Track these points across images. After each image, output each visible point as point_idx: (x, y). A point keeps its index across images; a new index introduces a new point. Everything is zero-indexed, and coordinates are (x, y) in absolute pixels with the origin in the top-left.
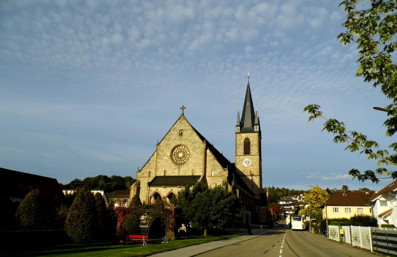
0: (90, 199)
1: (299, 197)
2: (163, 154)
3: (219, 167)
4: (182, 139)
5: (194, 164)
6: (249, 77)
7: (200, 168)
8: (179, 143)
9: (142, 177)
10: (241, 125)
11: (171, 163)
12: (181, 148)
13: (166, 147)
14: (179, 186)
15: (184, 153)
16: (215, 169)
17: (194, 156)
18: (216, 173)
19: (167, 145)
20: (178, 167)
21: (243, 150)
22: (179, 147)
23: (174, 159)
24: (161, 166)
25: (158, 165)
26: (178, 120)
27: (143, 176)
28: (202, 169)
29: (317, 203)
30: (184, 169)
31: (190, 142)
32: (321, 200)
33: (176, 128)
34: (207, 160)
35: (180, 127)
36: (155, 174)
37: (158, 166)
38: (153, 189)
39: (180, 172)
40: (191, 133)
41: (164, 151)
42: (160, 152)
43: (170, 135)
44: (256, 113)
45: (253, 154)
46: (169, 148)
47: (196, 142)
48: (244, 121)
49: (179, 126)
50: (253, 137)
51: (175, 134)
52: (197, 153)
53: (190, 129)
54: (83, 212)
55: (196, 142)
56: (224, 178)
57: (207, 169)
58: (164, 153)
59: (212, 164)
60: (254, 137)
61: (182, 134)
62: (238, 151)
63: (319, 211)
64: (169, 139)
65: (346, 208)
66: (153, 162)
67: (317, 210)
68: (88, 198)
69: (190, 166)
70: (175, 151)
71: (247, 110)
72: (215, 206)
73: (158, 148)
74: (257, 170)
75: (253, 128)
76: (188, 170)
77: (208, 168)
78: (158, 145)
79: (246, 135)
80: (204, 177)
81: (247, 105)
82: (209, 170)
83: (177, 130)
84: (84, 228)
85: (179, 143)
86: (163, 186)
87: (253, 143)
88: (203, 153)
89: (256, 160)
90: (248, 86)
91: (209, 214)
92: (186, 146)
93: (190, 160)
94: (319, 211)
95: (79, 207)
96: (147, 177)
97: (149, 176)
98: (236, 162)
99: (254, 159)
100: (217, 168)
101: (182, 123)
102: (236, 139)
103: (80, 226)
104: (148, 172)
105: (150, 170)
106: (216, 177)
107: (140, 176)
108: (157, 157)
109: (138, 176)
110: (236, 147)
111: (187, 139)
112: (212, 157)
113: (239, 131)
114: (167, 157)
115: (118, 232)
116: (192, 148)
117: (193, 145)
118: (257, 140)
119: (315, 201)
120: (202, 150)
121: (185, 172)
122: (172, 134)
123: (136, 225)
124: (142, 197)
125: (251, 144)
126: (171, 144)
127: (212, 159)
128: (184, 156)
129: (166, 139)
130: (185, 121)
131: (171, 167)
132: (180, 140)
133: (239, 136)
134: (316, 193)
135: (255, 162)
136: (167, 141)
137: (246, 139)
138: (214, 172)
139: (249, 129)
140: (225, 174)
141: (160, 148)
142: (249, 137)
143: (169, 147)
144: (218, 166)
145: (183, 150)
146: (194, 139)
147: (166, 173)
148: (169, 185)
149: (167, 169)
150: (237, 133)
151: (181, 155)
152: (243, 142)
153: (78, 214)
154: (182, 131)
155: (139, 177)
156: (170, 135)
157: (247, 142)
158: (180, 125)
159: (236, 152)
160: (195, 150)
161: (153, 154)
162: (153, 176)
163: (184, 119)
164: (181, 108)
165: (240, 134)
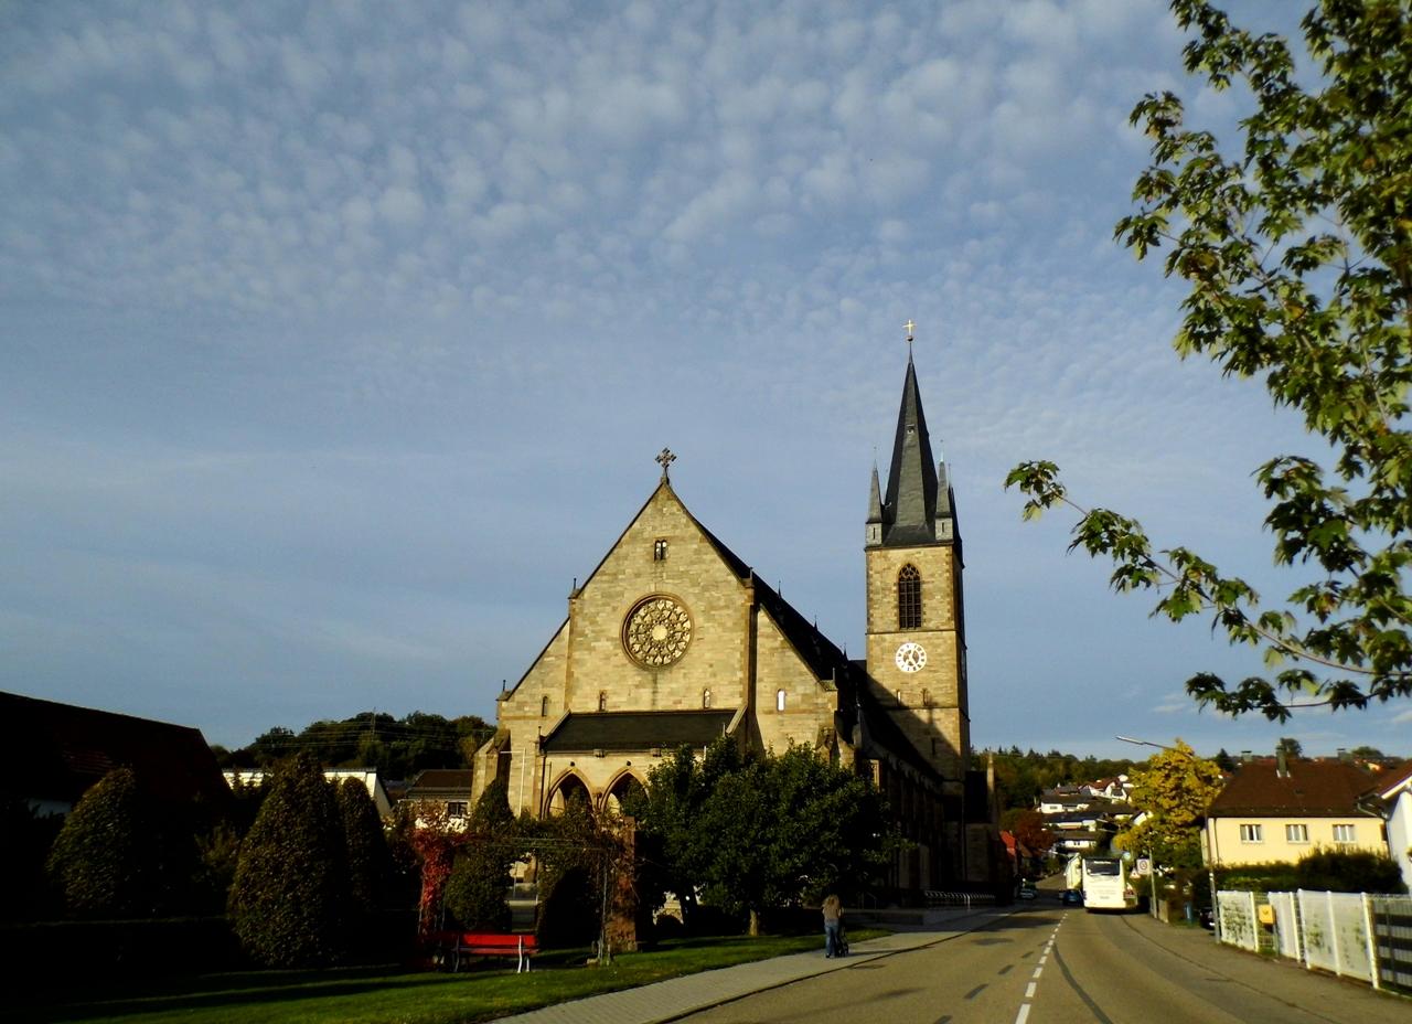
0: (321, 802)
1: (1113, 784)
2: (593, 631)
3: (803, 678)
4: (664, 575)
5: (711, 666)
6: (911, 340)
7: (731, 683)
8: (653, 590)
10: (887, 517)
12: (661, 606)
13: (604, 605)
14: (653, 751)
15: (672, 626)
16: (790, 684)
17: (707, 637)
18: (793, 698)
19: (607, 596)
20: (650, 677)
21: (896, 611)
22: (652, 605)
23: (637, 647)
24: (586, 675)
25: (577, 672)
26: (647, 504)
27: (519, 713)
29: (1178, 806)
30: (674, 686)
31: (693, 586)
32: (1197, 796)
33: (642, 533)
34: (760, 649)
35: (654, 528)
36: (566, 706)
37: (575, 675)
38: (560, 764)
39: (659, 696)
40: (697, 552)
41: (598, 619)
42: (580, 623)
43: (617, 559)
44: (942, 471)
45: (931, 625)
46: (614, 609)
47: (716, 585)
48: (895, 504)
49: (651, 527)
50: (931, 563)
51: (638, 553)
52: (722, 625)
53: (693, 537)
54: (294, 850)
55: (716, 585)
56: (822, 716)
57: (759, 686)
58: (598, 628)
59: (776, 666)
60: (937, 562)
61: (662, 556)
62: (876, 613)
63: (1188, 836)
64: (615, 574)
65: (1288, 826)
66: (558, 662)
67: (1181, 833)
68: (314, 797)
69: (696, 674)
70: (638, 620)
71: (905, 461)
72: (789, 821)
73: (574, 610)
74: (949, 685)
75: (933, 529)
76: (688, 689)
77: (761, 680)
78: (576, 597)
79: (907, 555)
80: (750, 716)
81: (908, 441)
82: (768, 689)
83: (645, 541)
84: (299, 912)
85: (652, 589)
86: (597, 752)
87: (930, 586)
88: (744, 624)
89: (943, 647)
90: (911, 374)
91: (767, 853)
92: (681, 600)
93: (694, 649)
94: (1188, 836)
95: (279, 834)
96: (535, 718)
97: (543, 715)
98: (868, 653)
99: (938, 646)
100: (797, 679)
102: (869, 569)
103: (283, 904)
104: (540, 698)
105: (546, 691)
106: (794, 712)
107: (511, 714)
108: (571, 642)
109: (503, 714)
110: (869, 599)
111: (681, 575)
112: (775, 638)
113: (878, 541)
114: (609, 643)
115: (423, 924)
116: (703, 608)
117: (707, 594)
118: (947, 571)
119: (1173, 798)
120: (739, 614)
123: (493, 897)
124: (517, 793)
125: (924, 586)
126: (622, 594)
128: (671, 637)
129: (604, 574)
130: (675, 508)
131: (624, 677)
132: (658, 577)
133: (879, 557)
134: (1176, 769)
135: (940, 655)
136: (608, 582)
137: (904, 569)
138: (786, 694)
139: (917, 532)
140: (826, 700)
141: (582, 609)
142: (915, 562)
143: (615, 605)
144: (801, 674)
145: (666, 613)
146: (707, 571)
147: (608, 701)
148: (619, 748)
149: (608, 688)
150: (869, 548)
151: (660, 633)
152: (895, 580)
153: (274, 859)
154: (664, 545)
155: (507, 719)
156: (617, 559)
157: (909, 579)
158: (657, 524)
159: (868, 619)
160: (713, 612)
161: (559, 632)
162: (557, 714)
163: (669, 499)
164: (659, 460)
165: (884, 552)
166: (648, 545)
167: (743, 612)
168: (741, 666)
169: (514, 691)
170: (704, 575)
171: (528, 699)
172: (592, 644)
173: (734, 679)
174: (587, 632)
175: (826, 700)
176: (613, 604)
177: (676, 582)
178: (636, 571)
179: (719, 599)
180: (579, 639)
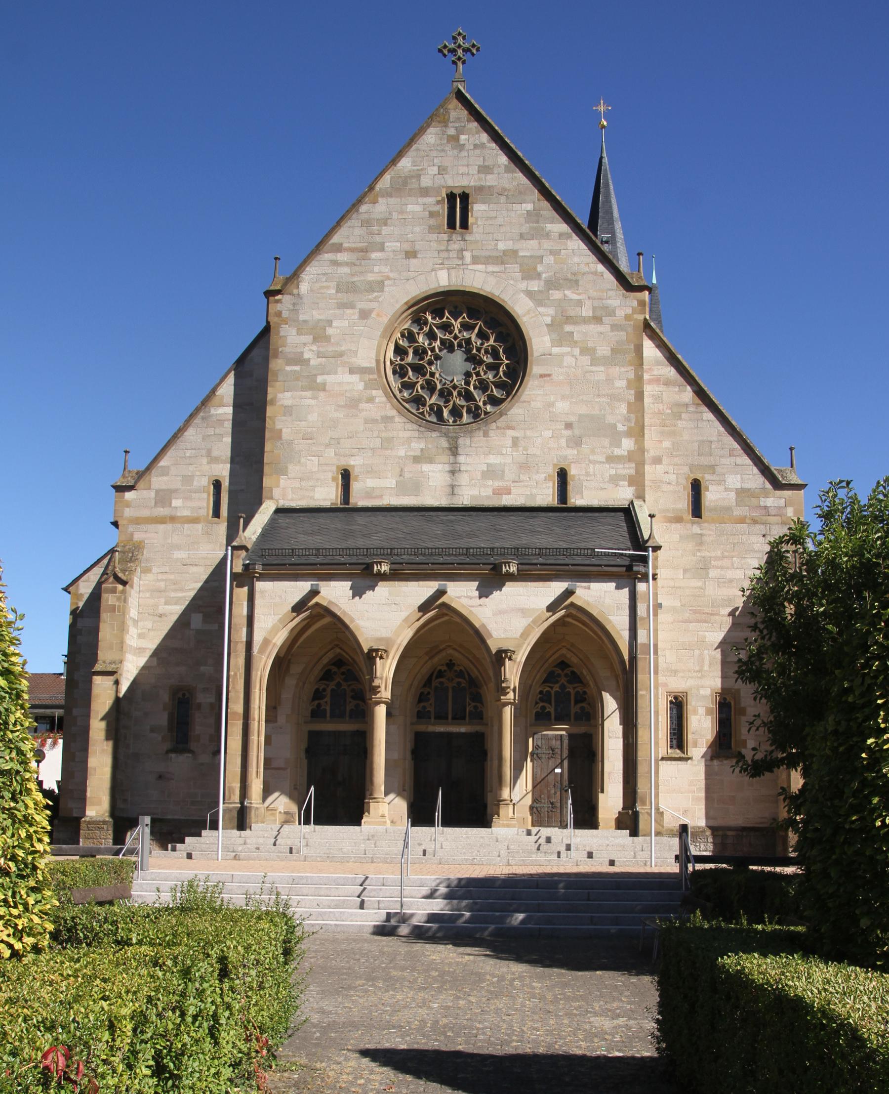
2: (319, 355)
4: (468, 255)
5: (569, 426)
7: (611, 459)
9: (161, 520)
11: (387, 419)
13: (343, 306)
17: (558, 374)
19: (347, 288)
20: (444, 443)
24: (308, 437)
27: (162, 511)
28: (630, 461)
30: (493, 459)
35: (442, 170)
39: (463, 479)
41: (330, 331)
46: (364, 315)
52: (585, 351)
76: (524, 467)
83: (425, 192)
85: (443, 280)
96: (194, 520)
100: (724, 461)
101: (462, 147)
107: (145, 513)
111: (504, 258)
114: (355, 378)
116: (548, 320)
117: (556, 295)
121: (497, 484)
122: (385, 222)
126: (379, 286)
127: (687, 405)
129: (339, 248)
131: (387, 443)
136: (347, 264)
141: (295, 310)
149: (355, 463)
155: (138, 521)
160: (568, 328)
166: (431, 200)
167: (630, 330)
168: (630, 428)
169: (149, 469)
170: (549, 260)
171: (177, 484)
172: (320, 379)
173: (617, 452)
174: (306, 356)
175: (782, 502)
176: (361, 305)
177: (491, 268)
178: (407, 247)
179: (579, 303)
180: (288, 368)
